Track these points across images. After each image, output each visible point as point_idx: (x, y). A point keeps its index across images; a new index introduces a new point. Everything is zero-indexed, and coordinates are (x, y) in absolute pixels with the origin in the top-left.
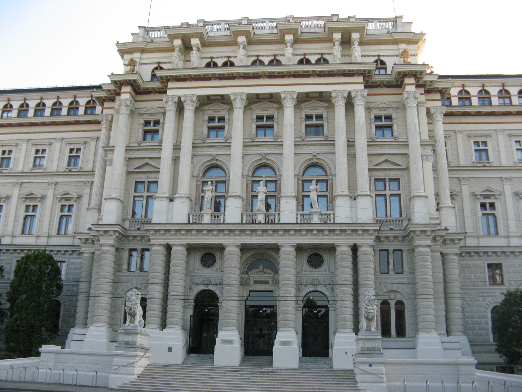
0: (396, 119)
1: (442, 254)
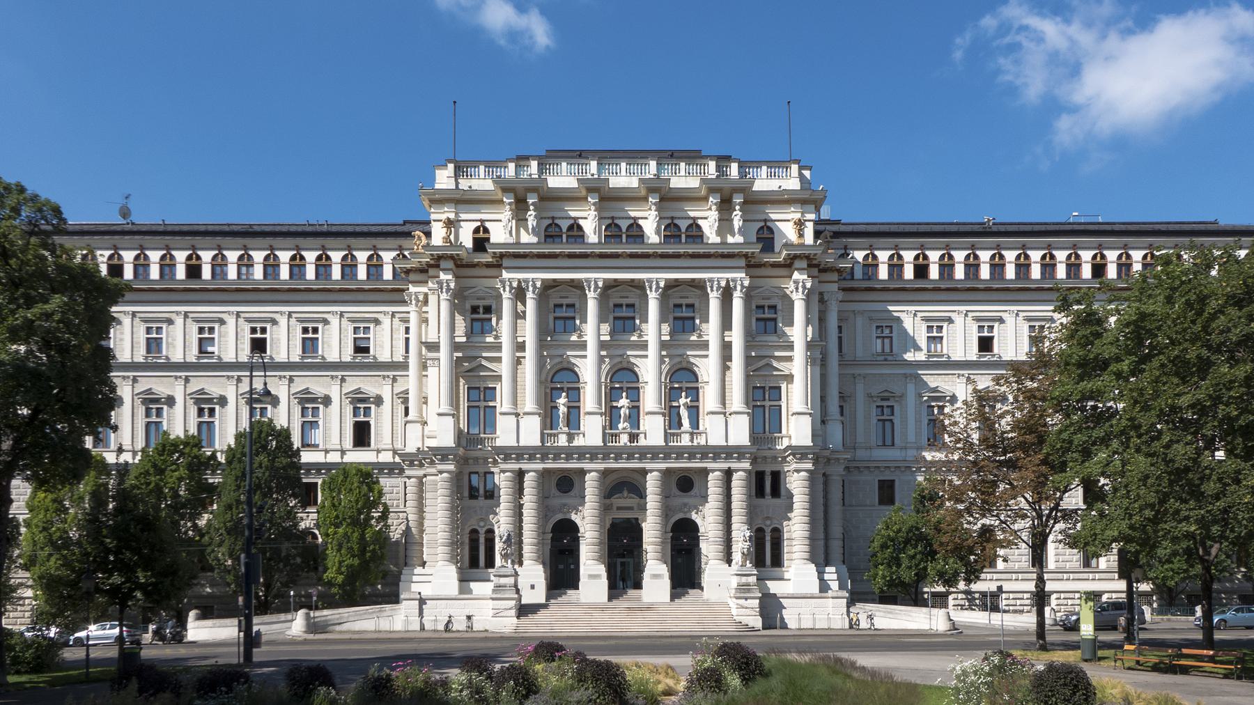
0: (782, 311)
1: (824, 474)
